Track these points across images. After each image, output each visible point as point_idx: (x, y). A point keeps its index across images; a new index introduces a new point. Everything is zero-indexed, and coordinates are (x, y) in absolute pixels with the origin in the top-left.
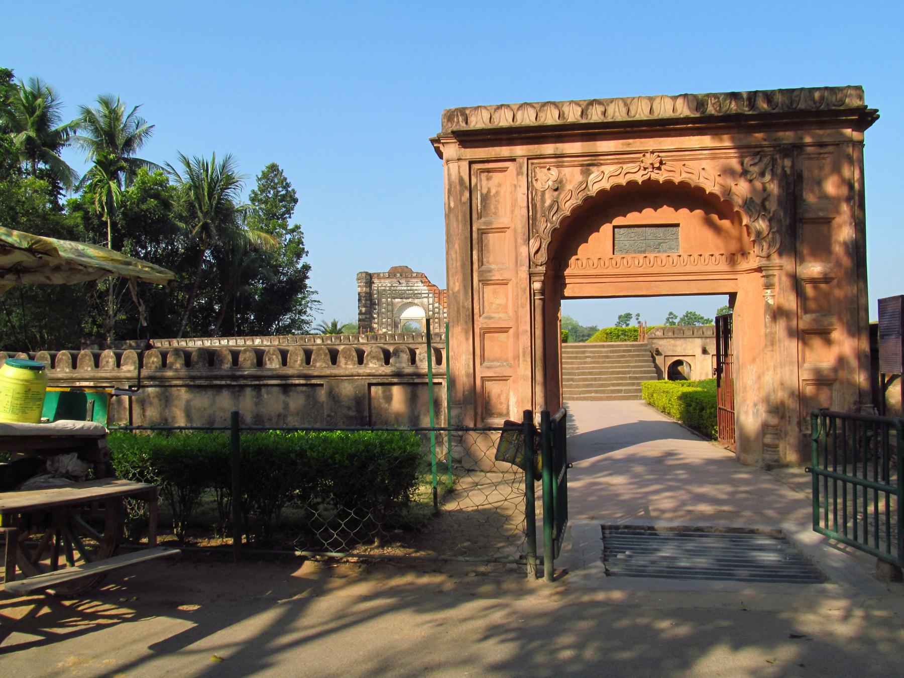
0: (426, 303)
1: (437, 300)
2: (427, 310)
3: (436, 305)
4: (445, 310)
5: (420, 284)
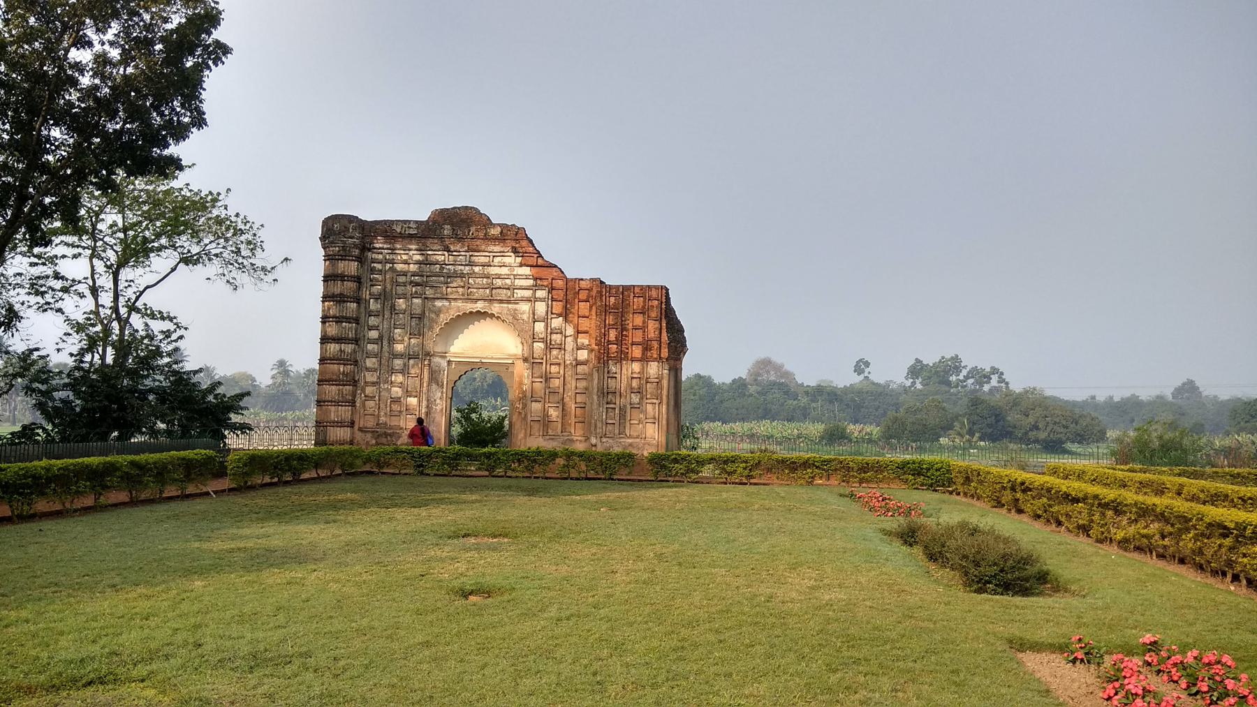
1: (558, 307)
3: (557, 322)
4: (584, 340)
5: (511, 259)
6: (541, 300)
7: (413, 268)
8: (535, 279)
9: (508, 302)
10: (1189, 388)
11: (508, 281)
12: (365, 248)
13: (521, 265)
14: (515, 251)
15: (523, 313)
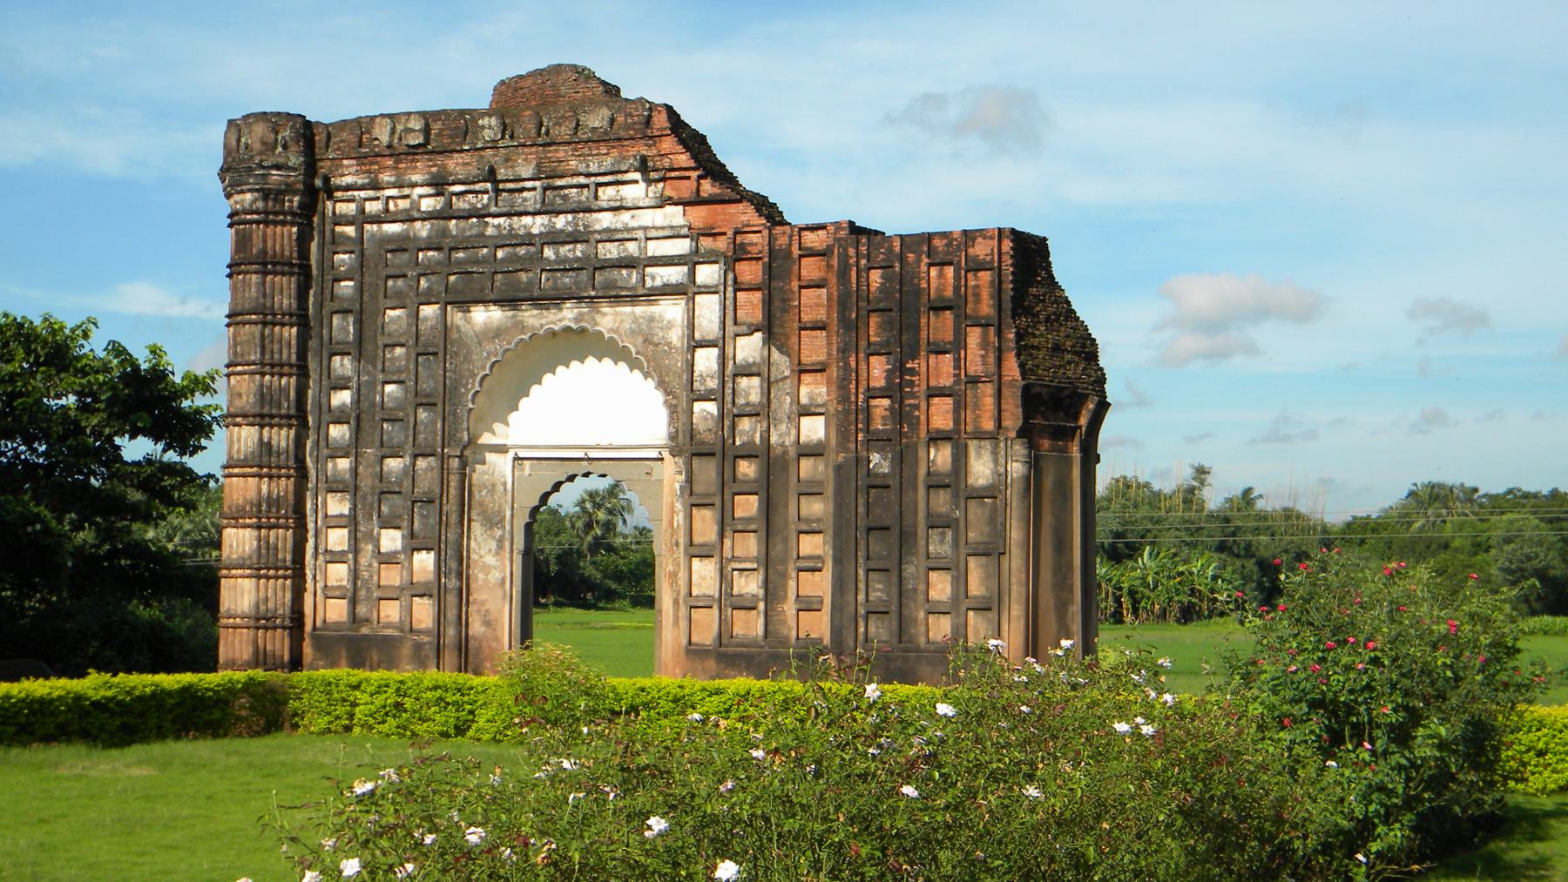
0: (676, 336)
1: (751, 305)
2: (681, 391)
3: (749, 348)
4: (813, 389)
5: (636, 191)
6: (708, 290)
7: (423, 229)
8: (695, 234)
9: (634, 299)
10: (540, 383)
11: (632, 248)
12: (315, 192)
13: (663, 201)
14: (644, 166)
15: (670, 325)
